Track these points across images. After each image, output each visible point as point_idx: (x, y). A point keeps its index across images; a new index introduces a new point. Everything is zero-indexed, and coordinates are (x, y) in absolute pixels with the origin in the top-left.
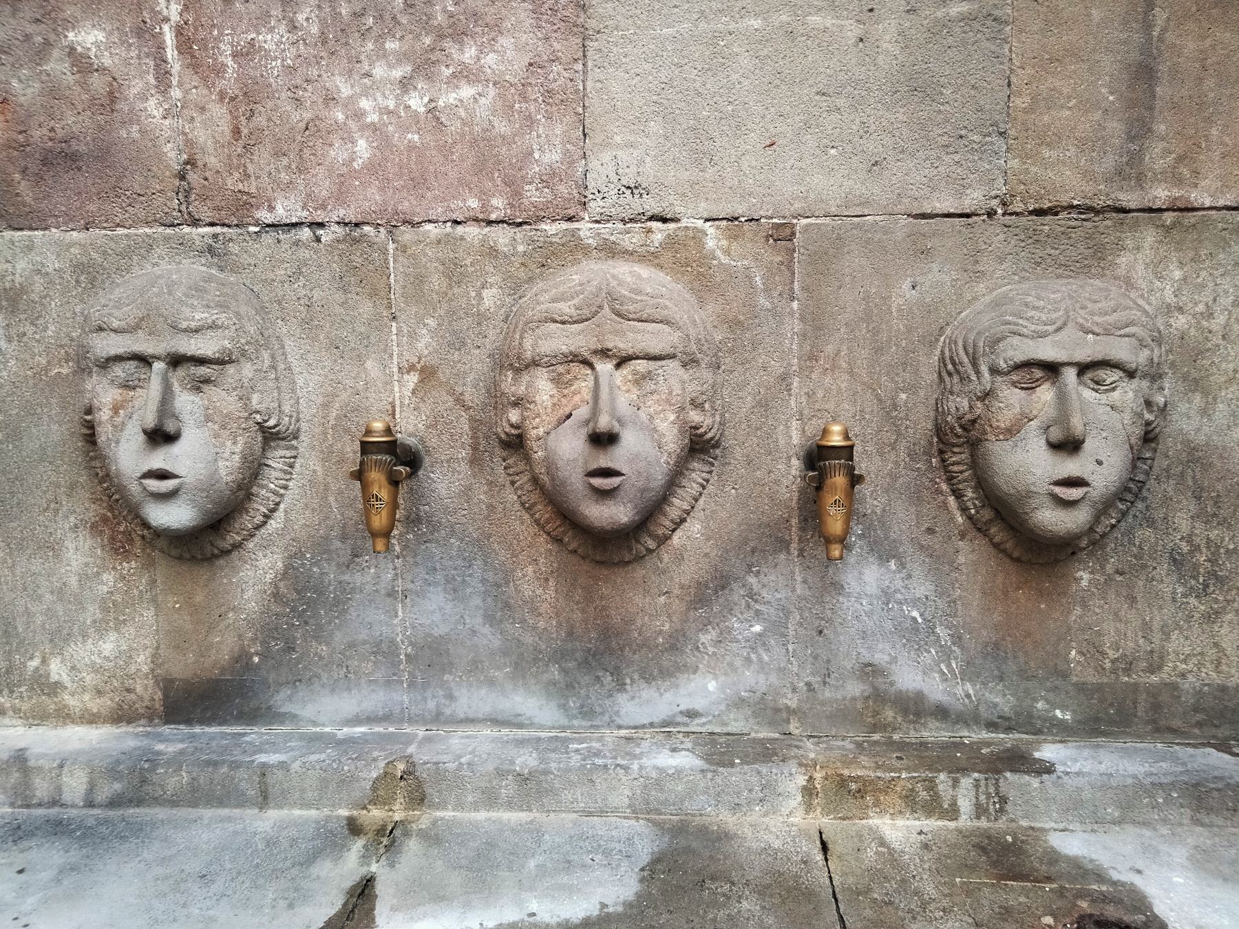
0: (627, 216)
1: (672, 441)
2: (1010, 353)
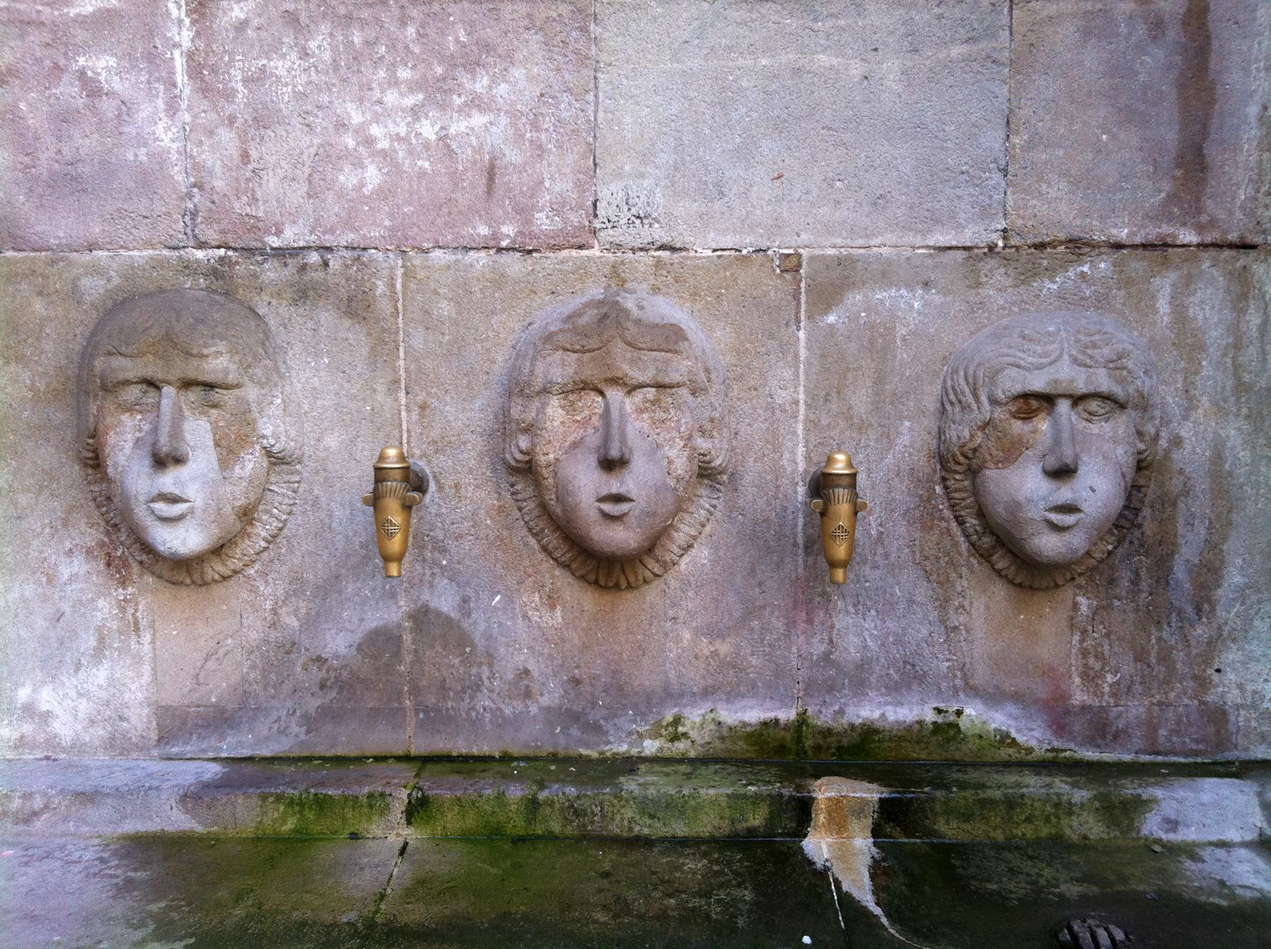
0: (637, 245)
1: (681, 465)
2: (1008, 384)
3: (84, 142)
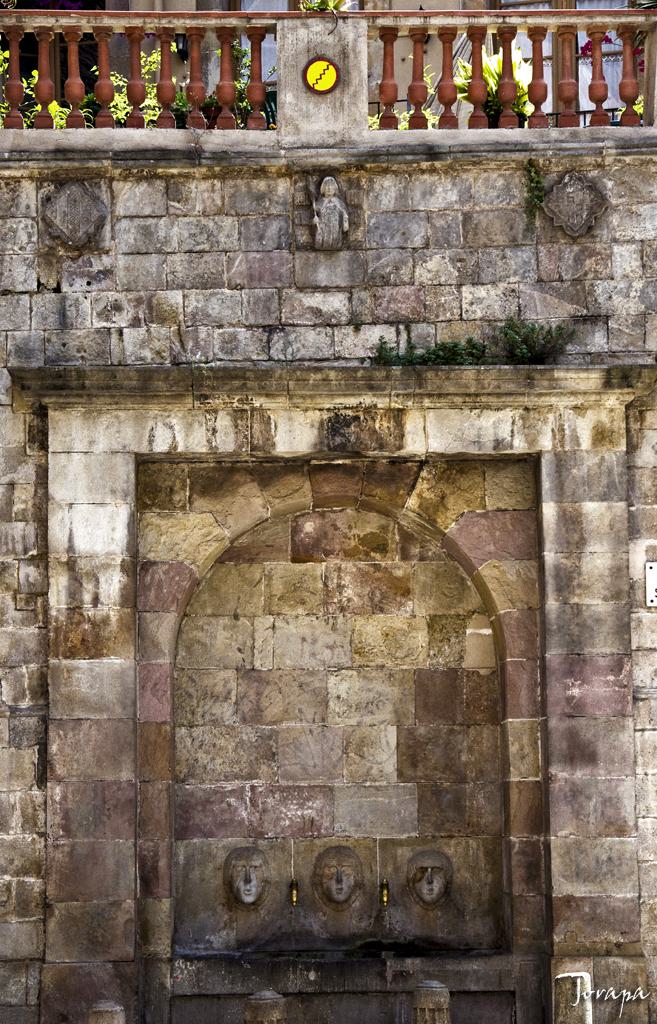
3: (227, 816)
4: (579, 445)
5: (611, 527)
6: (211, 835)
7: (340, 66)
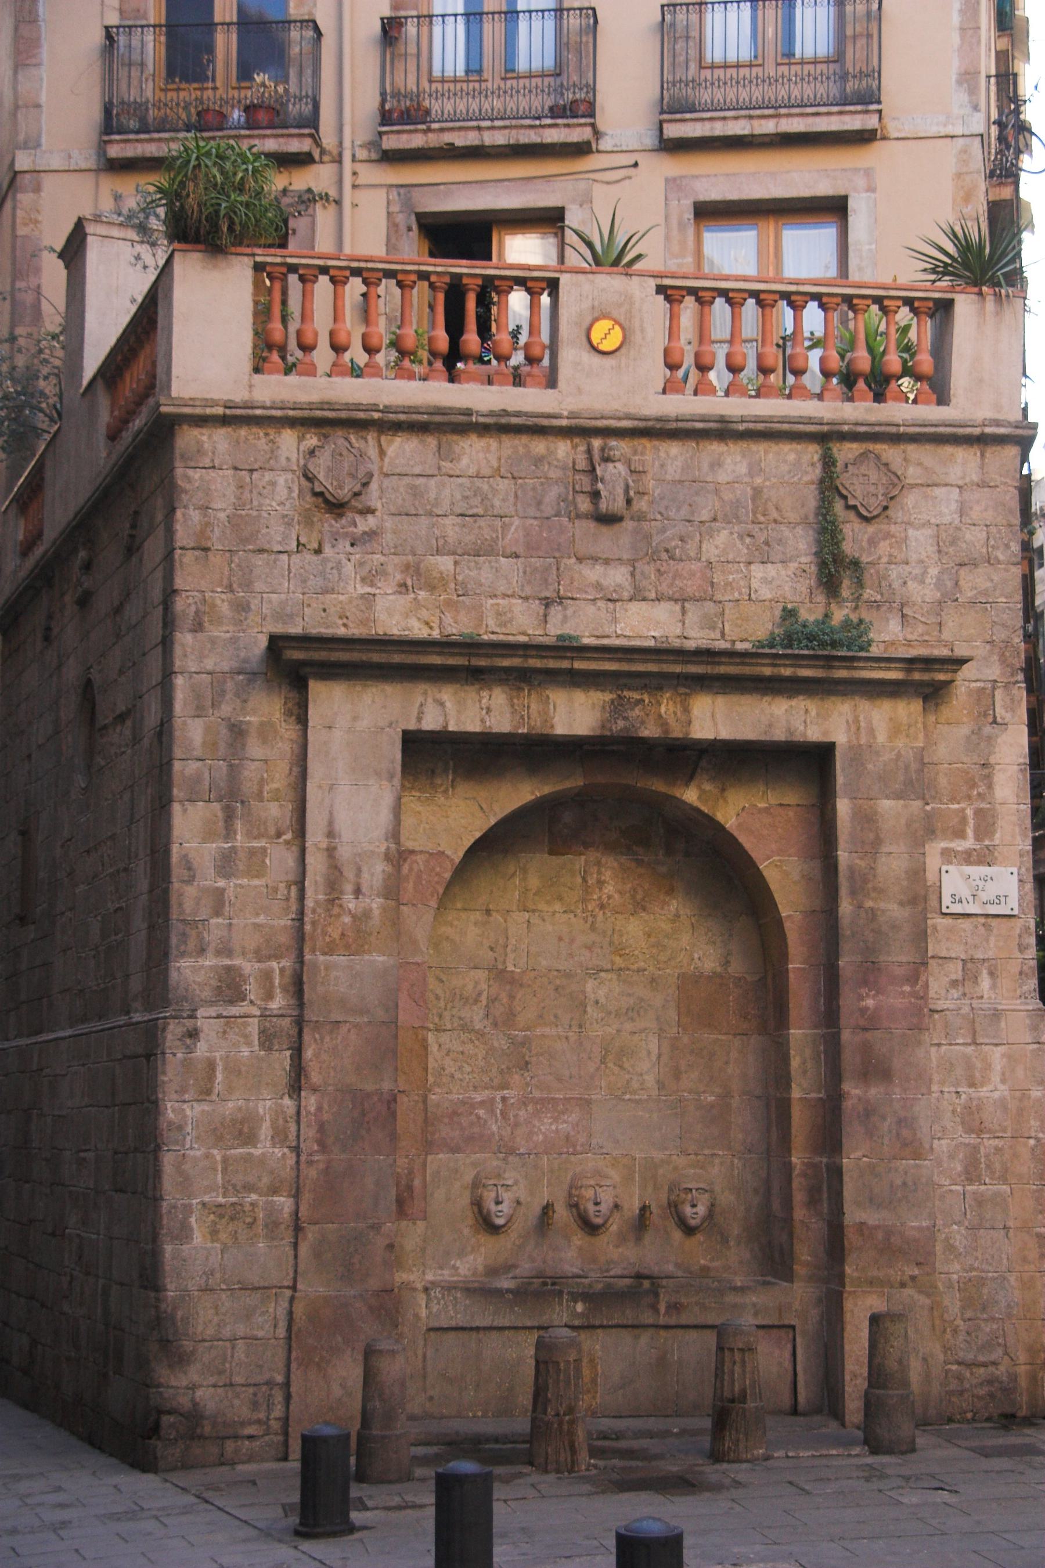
3: (476, 1130)
4: (875, 738)
5: (908, 825)
6: (455, 1150)
7: (626, 325)
